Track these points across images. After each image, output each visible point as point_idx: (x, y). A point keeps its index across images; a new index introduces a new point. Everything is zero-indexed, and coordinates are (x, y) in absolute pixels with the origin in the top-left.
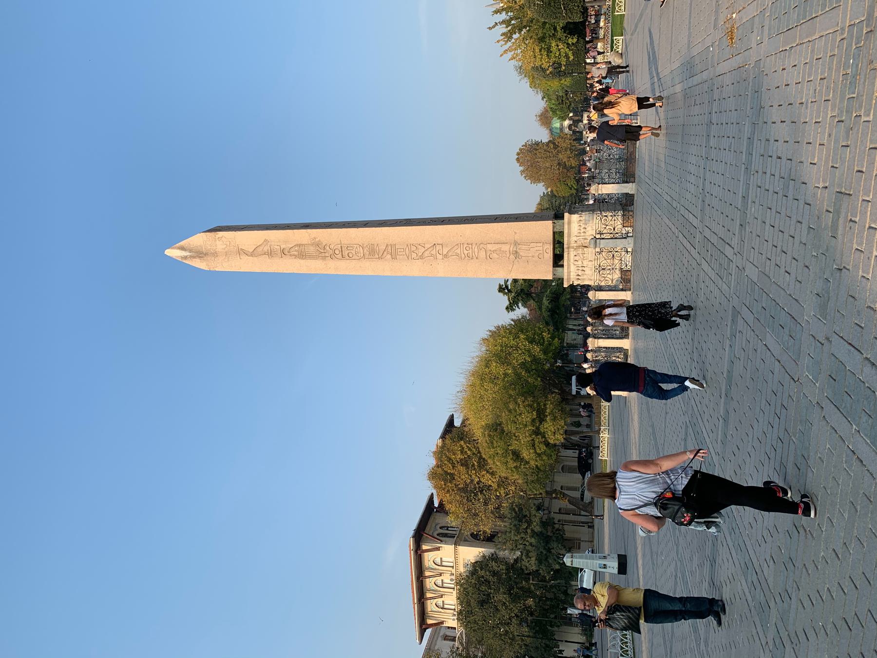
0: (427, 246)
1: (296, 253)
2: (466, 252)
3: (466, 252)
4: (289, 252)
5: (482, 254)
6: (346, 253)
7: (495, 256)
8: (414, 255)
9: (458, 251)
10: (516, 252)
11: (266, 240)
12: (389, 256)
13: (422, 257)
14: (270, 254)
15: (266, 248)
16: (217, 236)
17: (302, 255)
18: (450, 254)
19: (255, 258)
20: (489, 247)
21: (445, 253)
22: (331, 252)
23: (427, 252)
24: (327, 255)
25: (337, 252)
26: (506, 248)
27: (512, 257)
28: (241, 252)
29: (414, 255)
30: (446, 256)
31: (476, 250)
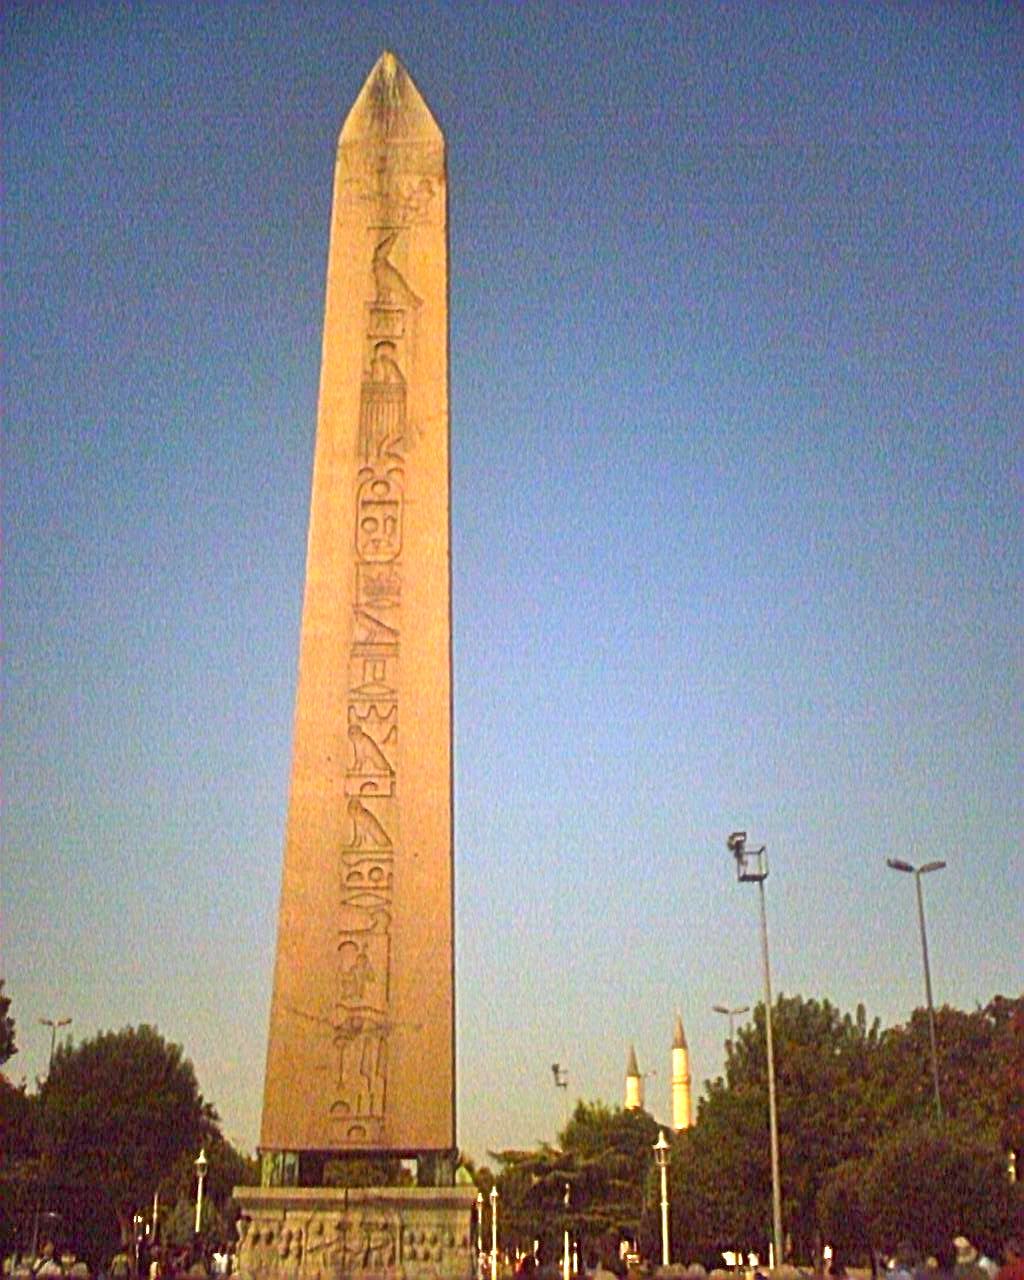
0: (388, 750)
1: (380, 378)
2: (365, 869)
3: (365, 869)
4: (383, 357)
6: (377, 512)
8: (362, 710)
9: (368, 845)
10: (358, 1030)
11: (419, 302)
12: (361, 635)
13: (354, 731)
14: (379, 309)
15: (396, 299)
16: (435, 181)
17: (372, 393)
19: (368, 267)
20: (378, 943)
21: (365, 803)
22: (380, 473)
23: (369, 748)
24: (373, 459)
25: (380, 488)
27: (342, 1017)
28: (386, 235)
29: (362, 710)
30: (355, 805)
31: (370, 901)
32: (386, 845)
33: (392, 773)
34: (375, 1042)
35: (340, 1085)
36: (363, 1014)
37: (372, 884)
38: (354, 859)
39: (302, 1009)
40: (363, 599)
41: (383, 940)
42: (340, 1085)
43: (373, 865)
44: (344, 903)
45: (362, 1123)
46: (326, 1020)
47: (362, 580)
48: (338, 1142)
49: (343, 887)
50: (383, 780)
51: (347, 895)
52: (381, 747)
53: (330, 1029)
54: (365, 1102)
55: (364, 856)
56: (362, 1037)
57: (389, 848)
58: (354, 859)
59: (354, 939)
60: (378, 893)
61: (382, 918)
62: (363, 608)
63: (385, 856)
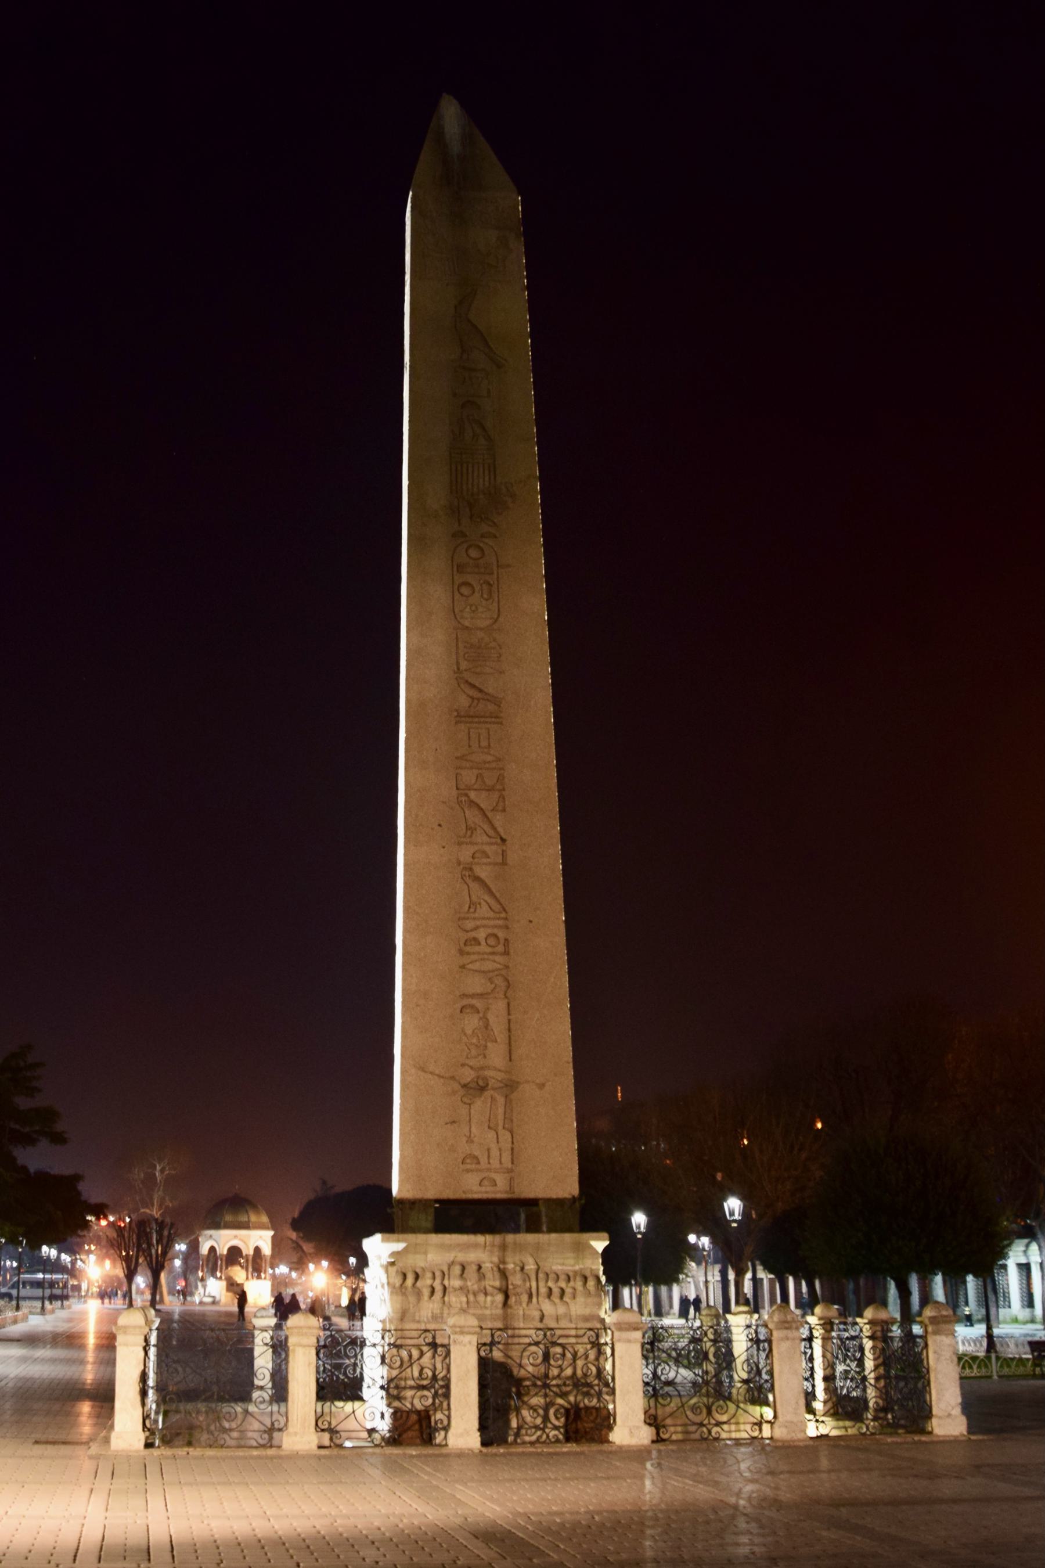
0: (498, 820)
2: (481, 935)
3: (481, 935)
5: (476, 984)
7: (471, 1022)
8: (469, 777)
9: (484, 911)
10: (482, 1089)
18: (474, 886)
20: (499, 1006)
26: (496, 1056)
27: (468, 1075)
30: (468, 873)
31: (489, 966)
32: (500, 913)
33: (503, 840)
34: (501, 1100)
35: (470, 1140)
36: (486, 1073)
37: (489, 950)
38: (469, 925)
39: (431, 1068)
40: (464, 665)
41: (502, 1005)
42: (470, 1140)
43: (490, 931)
44: (463, 967)
45: (493, 1175)
46: (453, 1078)
47: (461, 645)
48: (472, 1191)
49: (461, 952)
50: (494, 847)
51: (466, 960)
52: (489, 814)
53: (457, 1086)
54: (495, 1153)
55: (478, 923)
56: (488, 1093)
57: (503, 915)
58: (469, 925)
59: (474, 1002)
60: (497, 958)
61: (499, 981)
62: (466, 675)
63: (501, 922)
